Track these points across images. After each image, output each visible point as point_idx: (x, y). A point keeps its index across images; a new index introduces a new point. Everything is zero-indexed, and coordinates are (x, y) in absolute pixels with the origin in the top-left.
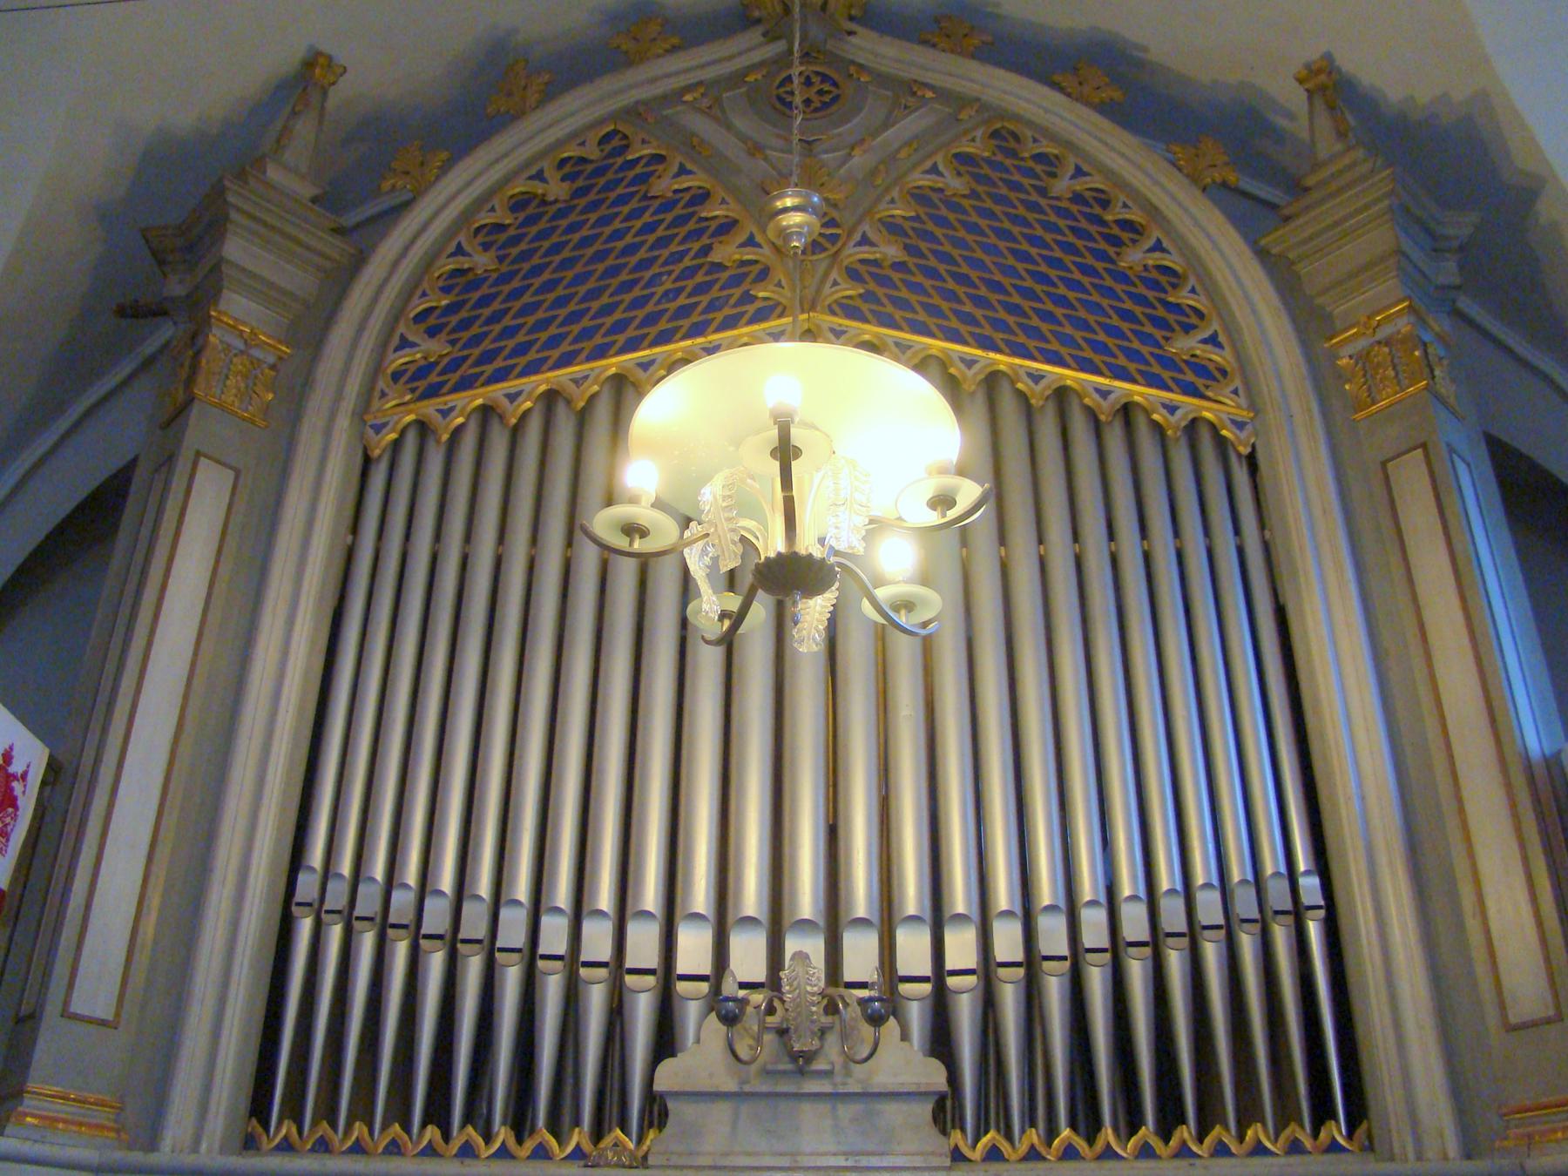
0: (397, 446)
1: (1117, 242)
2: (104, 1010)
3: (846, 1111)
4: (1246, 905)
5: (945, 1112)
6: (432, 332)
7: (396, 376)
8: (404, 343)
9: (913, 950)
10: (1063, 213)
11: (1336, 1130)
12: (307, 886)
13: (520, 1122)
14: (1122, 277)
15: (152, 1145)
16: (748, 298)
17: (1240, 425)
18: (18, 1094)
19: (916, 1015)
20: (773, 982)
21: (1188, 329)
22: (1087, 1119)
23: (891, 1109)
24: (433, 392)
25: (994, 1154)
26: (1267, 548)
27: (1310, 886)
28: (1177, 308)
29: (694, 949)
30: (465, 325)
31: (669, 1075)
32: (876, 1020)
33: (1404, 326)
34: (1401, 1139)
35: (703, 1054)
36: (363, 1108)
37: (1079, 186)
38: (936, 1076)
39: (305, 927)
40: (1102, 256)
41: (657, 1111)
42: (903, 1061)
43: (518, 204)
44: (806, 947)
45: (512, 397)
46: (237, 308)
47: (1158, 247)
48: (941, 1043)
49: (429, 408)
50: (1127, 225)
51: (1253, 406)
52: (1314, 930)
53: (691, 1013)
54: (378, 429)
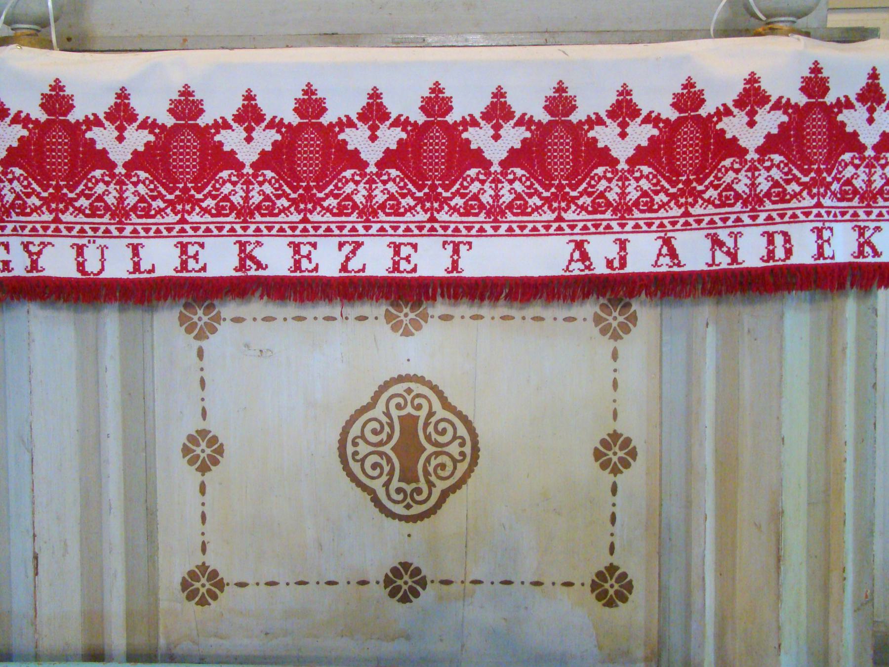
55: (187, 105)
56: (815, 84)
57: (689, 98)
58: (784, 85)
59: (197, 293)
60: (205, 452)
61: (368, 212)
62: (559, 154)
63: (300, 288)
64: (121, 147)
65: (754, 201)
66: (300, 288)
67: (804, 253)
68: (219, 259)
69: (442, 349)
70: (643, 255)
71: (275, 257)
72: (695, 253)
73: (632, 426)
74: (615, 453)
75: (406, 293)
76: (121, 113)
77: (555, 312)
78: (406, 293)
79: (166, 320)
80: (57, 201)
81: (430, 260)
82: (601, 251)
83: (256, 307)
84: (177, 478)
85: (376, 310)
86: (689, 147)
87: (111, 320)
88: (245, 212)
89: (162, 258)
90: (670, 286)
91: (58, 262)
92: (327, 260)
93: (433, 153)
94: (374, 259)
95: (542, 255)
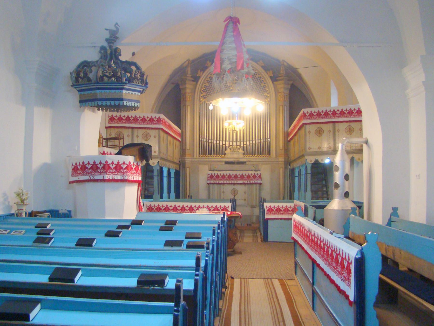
1: (261, 82)
4: (264, 140)
6: (204, 92)
8: (202, 93)
9: (242, 143)
10: (257, 79)
12: (201, 139)
13: (217, 154)
14: (261, 86)
15: (193, 156)
19: (242, 148)
20: (233, 145)
22: (252, 155)
27: (269, 140)
29: (227, 143)
30: (206, 91)
31: (226, 152)
33: (283, 94)
35: (228, 151)
37: (259, 76)
38: (243, 152)
40: (260, 84)
41: (225, 154)
42: (241, 151)
43: (210, 77)
44: (235, 144)
46: (188, 91)
47: (265, 83)
48: (243, 150)
49: (205, 100)
50: (263, 80)
55: (224, 174)
58: (253, 174)
59: (224, 184)
60: (223, 192)
62: (242, 177)
63: (229, 184)
64: (220, 176)
66: (229, 184)
68: (225, 182)
70: (246, 182)
71: (228, 182)
72: (249, 182)
74: (245, 193)
75: (234, 184)
76: (220, 175)
78: (234, 184)
79: (222, 186)
81: (236, 182)
82: (244, 182)
84: (222, 193)
86: (249, 177)
87: (219, 185)
89: (222, 182)
90: (248, 184)
91: (217, 182)
92: (230, 182)
93: (236, 177)
94: (233, 182)
95: (241, 182)
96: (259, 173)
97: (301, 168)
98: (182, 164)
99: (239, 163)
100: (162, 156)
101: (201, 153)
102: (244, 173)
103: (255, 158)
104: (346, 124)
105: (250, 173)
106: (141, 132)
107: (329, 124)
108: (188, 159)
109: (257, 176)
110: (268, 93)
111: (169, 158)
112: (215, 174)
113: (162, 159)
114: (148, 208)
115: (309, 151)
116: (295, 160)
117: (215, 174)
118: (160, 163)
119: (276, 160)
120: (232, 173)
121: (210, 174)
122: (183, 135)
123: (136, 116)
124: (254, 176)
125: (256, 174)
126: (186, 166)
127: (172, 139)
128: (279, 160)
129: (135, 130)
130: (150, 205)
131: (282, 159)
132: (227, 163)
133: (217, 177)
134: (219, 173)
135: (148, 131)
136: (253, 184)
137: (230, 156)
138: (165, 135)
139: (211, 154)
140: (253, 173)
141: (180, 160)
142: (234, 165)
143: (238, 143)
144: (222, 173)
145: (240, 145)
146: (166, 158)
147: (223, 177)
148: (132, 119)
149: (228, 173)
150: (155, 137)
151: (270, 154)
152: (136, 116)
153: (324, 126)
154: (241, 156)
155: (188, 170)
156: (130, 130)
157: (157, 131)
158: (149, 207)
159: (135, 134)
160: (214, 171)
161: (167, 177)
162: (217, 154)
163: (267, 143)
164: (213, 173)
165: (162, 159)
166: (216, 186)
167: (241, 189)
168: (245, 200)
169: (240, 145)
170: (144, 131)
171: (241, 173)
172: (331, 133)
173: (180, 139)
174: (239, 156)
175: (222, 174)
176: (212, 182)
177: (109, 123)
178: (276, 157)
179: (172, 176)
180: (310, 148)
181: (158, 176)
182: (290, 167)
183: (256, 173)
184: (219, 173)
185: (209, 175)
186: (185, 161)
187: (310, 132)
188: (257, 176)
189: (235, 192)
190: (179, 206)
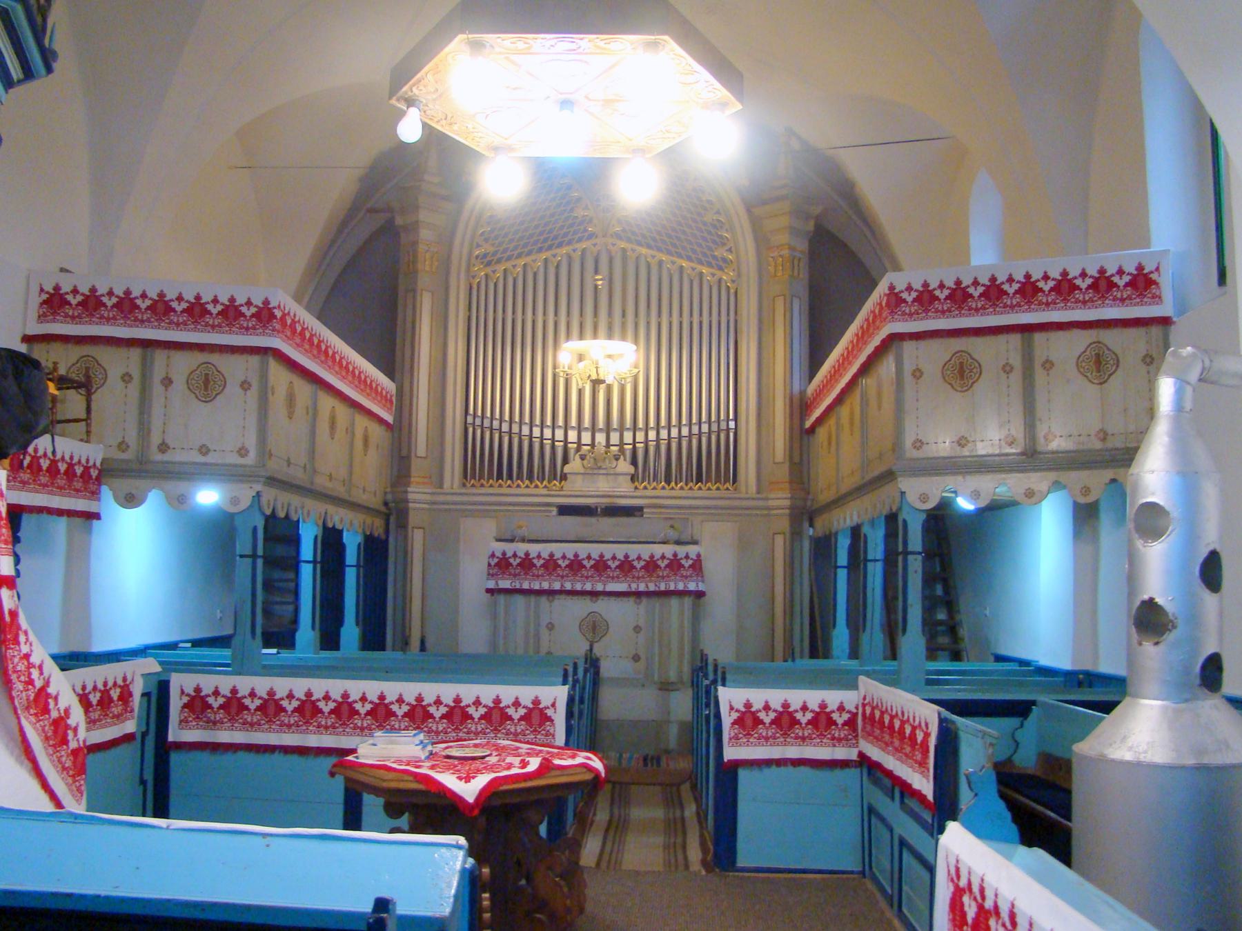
0: (479, 283)
2: (424, 455)
3: (610, 478)
4: (714, 427)
5: (633, 478)
7: (477, 257)
8: (478, 246)
9: (628, 437)
11: (727, 485)
12: (470, 419)
13: (530, 478)
15: (441, 486)
16: (586, 230)
17: (733, 281)
18: (410, 477)
19: (628, 454)
20: (593, 445)
21: (724, 244)
22: (668, 481)
23: (621, 478)
24: (489, 264)
25: (645, 488)
26: (736, 321)
27: (732, 425)
28: (721, 237)
31: (567, 469)
32: (617, 459)
33: (786, 252)
34: (743, 489)
35: (575, 465)
36: (490, 476)
38: (632, 470)
39: (471, 430)
41: (564, 477)
42: (624, 466)
44: (600, 438)
45: (514, 266)
48: (634, 462)
49: (489, 270)
51: (739, 275)
52: (732, 435)
53: (572, 452)
54: (474, 277)
56: (675, 555)
57: (652, 556)
58: (669, 555)
59: (551, 593)
60: (551, 627)
61: (587, 578)
62: (626, 566)
63: (572, 593)
65: (663, 577)
66: (572, 593)
67: (672, 588)
68: (557, 586)
69: (603, 607)
70: (642, 588)
71: (568, 586)
72: (652, 588)
73: (641, 623)
74: (637, 629)
75: (594, 594)
76: (539, 557)
77: (625, 599)
78: (594, 594)
79: (543, 599)
80: (526, 574)
81: (600, 587)
82: (634, 587)
83: (563, 597)
85: (588, 598)
86: (651, 566)
87: (533, 599)
88: (562, 577)
89: (545, 585)
90: (648, 594)
91: (526, 586)
92: (578, 587)
93: (601, 566)
94: (588, 587)
95: (621, 587)
96: (693, 550)
97: (866, 529)
98: (394, 513)
99: (613, 511)
100: (275, 466)
101: (471, 472)
102: (633, 551)
103: (677, 493)
104: (1082, 339)
105: (658, 550)
106: (183, 364)
107: (1002, 339)
108: (418, 494)
109: (687, 563)
110: (730, 250)
111: (321, 482)
112: (515, 555)
113: (272, 481)
114: (186, 699)
115: (916, 454)
116: (840, 501)
117: (515, 555)
118: (264, 500)
119: (761, 503)
120: (583, 550)
121: (499, 554)
122: (402, 403)
123: (162, 295)
124: (675, 564)
125: (681, 555)
126: (413, 519)
127: (342, 411)
128: (771, 503)
129: (160, 356)
130: (198, 690)
131: (781, 499)
132: (565, 510)
133: (527, 564)
134: (534, 549)
135: (215, 358)
136: (667, 594)
137: (582, 487)
138: (304, 390)
139: (510, 477)
140: (668, 550)
141: (389, 497)
142: (593, 520)
143: (615, 438)
144: (545, 550)
145: (621, 444)
146: (308, 486)
147: (551, 565)
148: (144, 304)
149: (570, 549)
150: (245, 386)
151: (735, 481)
152: (162, 295)
153: (981, 348)
154: (625, 486)
155: (417, 540)
156: (135, 354)
157: (255, 360)
158: (193, 699)
159: (158, 373)
160: (512, 541)
161: (314, 562)
162: (530, 478)
163: (722, 436)
164: (509, 548)
165: (272, 481)
166: (520, 600)
167: (620, 614)
168: (636, 658)
169: (621, 444)
170: (198, 358)
171: (620, 551)
172: (1016, 376)
173: (389, 418)
174: (616, 485)
175: (545, 555)
176: (505, 584)
177: (42, 318)
178: (758, 493)
179: (351, 557)
180: (919, 444)
181: (254, 556)
182: (811, 532)
183: (681, 551)
184: (534, 549)
185: (493, 555)
186: (407, 501)
187: (918, 374)
188: (687, 563)
189: (594, 628)
190: (327, 697)
